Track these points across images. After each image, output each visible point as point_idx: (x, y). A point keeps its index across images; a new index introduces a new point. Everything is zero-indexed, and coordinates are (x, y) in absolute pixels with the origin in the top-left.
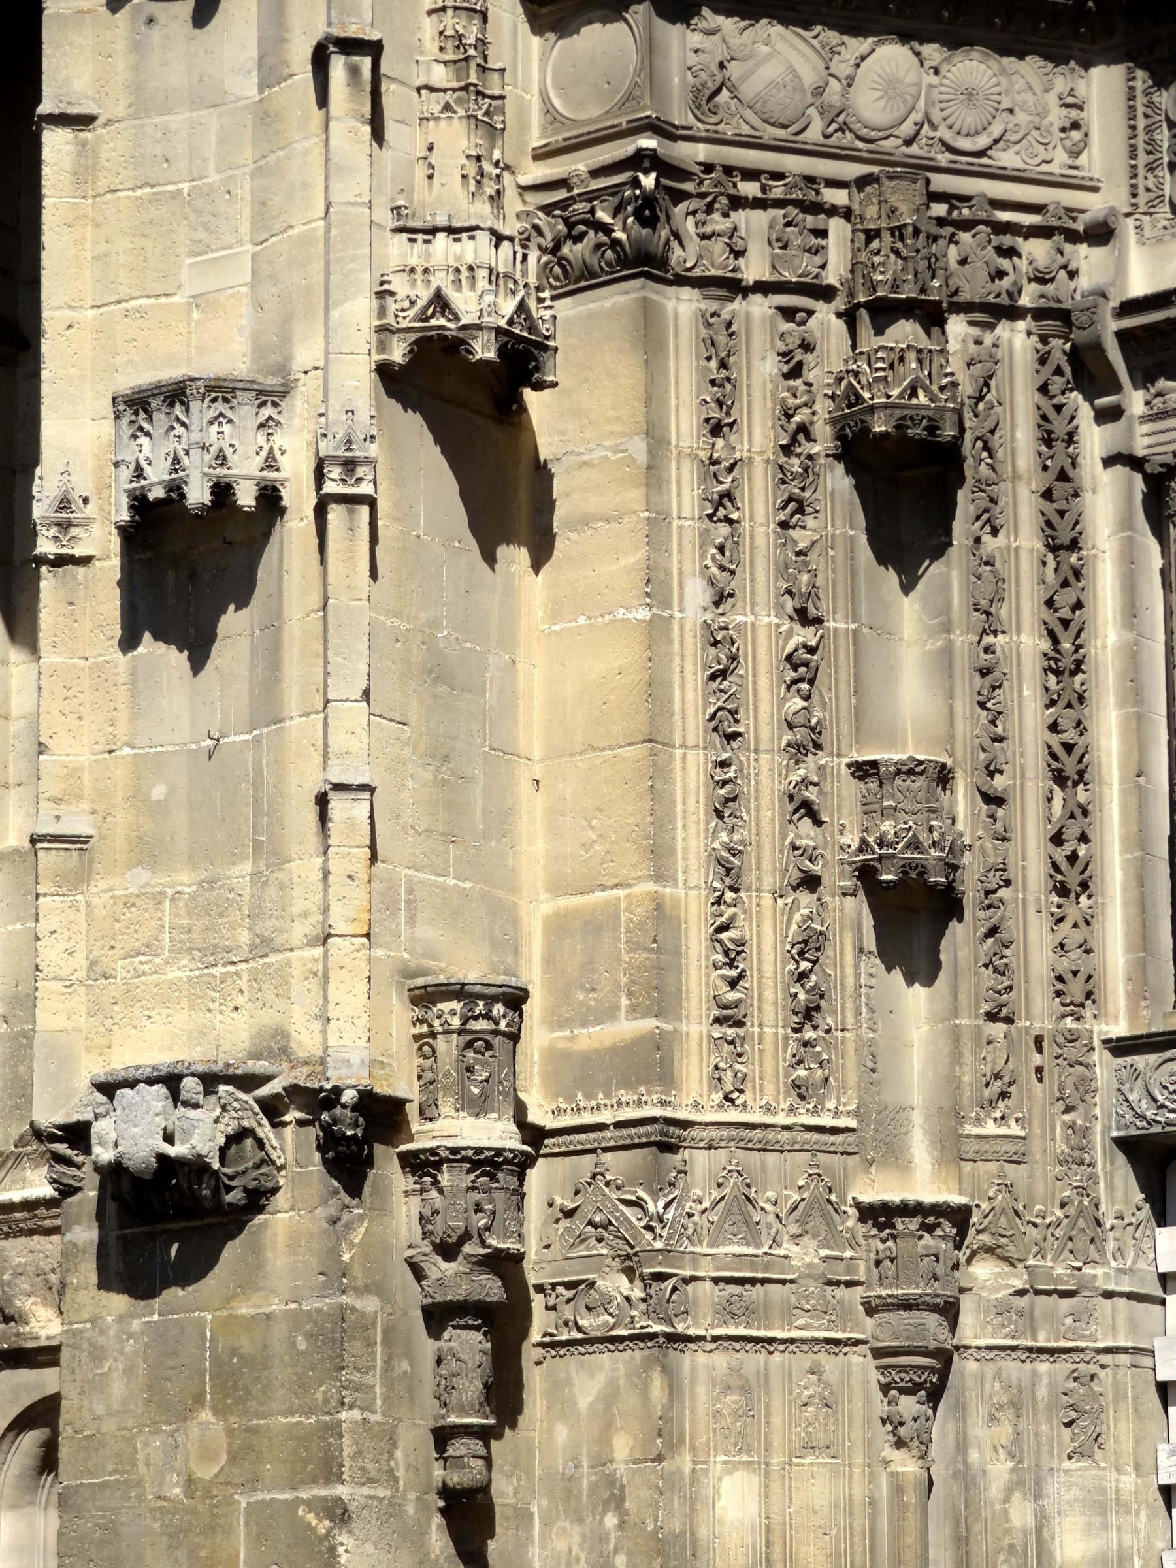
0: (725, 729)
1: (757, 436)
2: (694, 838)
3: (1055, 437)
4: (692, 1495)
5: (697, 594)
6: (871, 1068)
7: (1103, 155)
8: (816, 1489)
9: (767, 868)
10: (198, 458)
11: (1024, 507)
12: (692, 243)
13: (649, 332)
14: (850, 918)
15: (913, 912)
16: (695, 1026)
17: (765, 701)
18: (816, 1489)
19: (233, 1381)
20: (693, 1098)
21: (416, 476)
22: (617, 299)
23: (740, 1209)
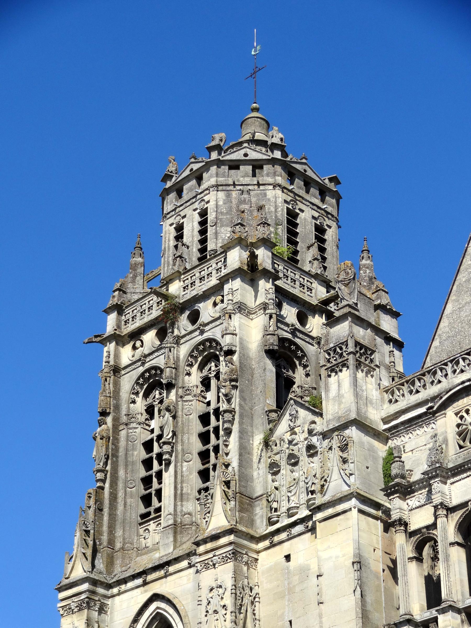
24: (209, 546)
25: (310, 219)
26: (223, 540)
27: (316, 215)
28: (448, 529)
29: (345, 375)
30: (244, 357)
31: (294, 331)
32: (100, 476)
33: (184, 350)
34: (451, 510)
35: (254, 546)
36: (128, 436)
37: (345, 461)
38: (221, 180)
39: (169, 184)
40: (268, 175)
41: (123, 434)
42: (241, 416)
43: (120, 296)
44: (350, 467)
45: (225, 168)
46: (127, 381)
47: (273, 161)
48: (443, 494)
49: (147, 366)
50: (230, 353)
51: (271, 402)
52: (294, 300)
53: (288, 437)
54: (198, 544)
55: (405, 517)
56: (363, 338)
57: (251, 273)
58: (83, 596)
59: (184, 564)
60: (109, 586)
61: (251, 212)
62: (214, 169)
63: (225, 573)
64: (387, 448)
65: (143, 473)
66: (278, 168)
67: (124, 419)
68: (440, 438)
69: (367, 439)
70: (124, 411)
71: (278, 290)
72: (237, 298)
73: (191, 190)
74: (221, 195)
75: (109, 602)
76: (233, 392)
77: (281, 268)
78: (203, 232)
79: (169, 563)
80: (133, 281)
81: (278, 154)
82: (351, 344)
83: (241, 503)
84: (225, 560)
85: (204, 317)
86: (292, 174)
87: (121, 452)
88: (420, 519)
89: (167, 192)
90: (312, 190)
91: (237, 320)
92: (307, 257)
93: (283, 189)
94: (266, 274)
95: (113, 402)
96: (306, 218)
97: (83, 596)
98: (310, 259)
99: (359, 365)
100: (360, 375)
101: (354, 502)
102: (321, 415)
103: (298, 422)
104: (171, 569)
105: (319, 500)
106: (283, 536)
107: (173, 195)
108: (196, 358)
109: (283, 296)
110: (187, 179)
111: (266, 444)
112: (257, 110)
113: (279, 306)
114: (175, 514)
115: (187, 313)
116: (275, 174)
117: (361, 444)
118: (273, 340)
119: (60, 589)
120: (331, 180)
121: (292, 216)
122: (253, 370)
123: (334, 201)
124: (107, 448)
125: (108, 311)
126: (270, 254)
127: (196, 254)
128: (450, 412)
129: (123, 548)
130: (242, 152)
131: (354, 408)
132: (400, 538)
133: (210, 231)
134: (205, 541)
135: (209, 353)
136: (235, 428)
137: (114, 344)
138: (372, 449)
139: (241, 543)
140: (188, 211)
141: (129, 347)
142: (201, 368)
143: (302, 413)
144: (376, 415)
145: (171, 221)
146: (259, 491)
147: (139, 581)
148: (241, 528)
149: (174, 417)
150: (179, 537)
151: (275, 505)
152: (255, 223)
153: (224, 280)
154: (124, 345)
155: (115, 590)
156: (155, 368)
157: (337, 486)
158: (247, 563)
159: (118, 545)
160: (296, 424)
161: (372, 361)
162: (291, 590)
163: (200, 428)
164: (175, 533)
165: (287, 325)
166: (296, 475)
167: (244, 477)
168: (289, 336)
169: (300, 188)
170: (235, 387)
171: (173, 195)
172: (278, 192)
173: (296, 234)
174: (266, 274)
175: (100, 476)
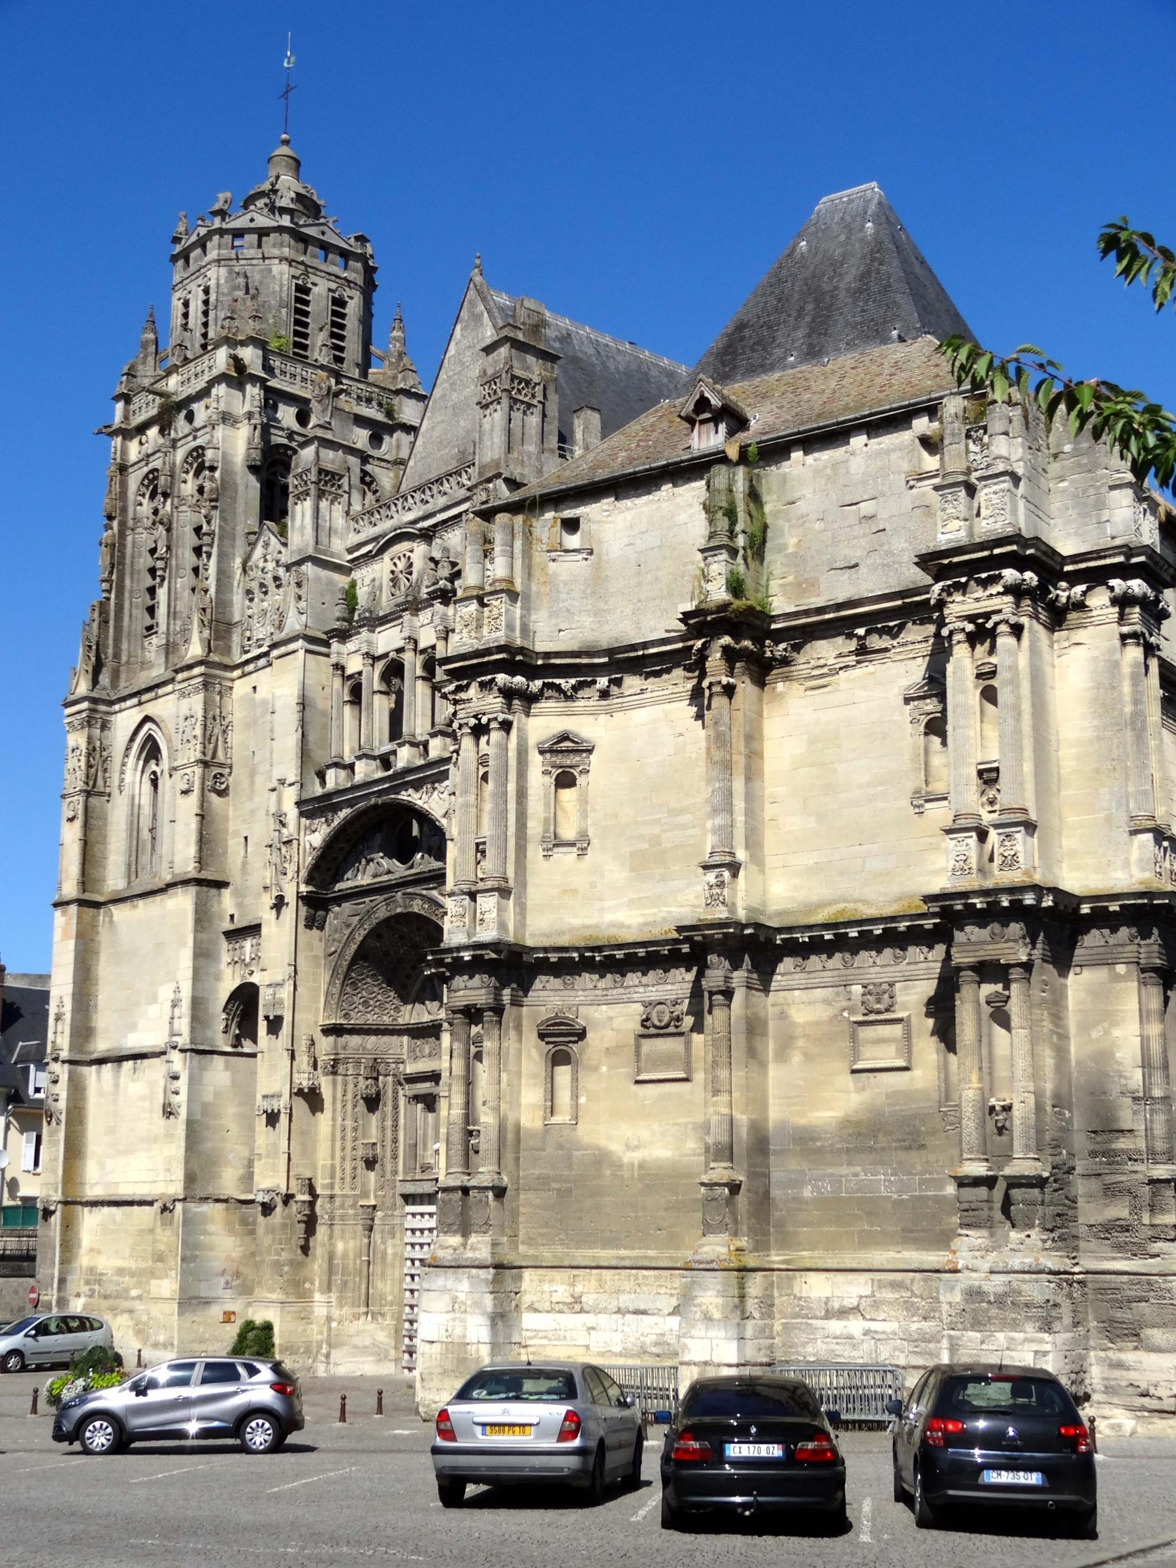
0: (343, 1138)
1: (350, 1096)
2: (338, 1154)
3: (395, 1092)
4: (332, 1245)
5: (339, 1120)
6: (363, 1185)
7: (405, 1050)
8: (352, 1244)
9: (348, 1159)
10: (267, 1105)
11: (390, 1103)
12: (341, 1069)
13: (334, 1083)
14: (361, 1165)
15: (370, 1164)
16: (337, 1180)
17: (349, 1134)
18: (352, 1244)
19: (273, 1231)
20: (337, 1191)
21: (301, 1106)
22: (330, 1077)
23: (342, 1206)
24: (185, 674)
25: (324, 292)
26: (197, 671)
27: (333, 286)
28: (373, 678)
29: (308, 504)
30: (228, 472)
31: (291, 435)
32: (105, 586)
33: (180, 454)
34: (375, 659)
35: (228, 675)
36: (134, 542)
37: (300, 598)
38: (224, 252)
39: (178, 248)
40: (274, 246)
41: (129, 539)
42: (221, 538)
43: (128, 381)
44: (303, 604)
45: (228, 238)
46: (134, 480)
47: (280, 229)
48: (369, 643)
49: (151, 466)
50: (212, 469)
51: (253, 522)
52: (291, 399)
53: (261, 564)
54: (176, 672)
55: (343, 662)
56: (333, 462)
57: (238, 376)
58: (84, 715)
59: (169, 688)
60: (111, 703)
61: (244, 300)
62: (216, 238)
63: (196, 703)
64: (349, 579)
65: (149, 582)
66: (286, 237)
67: (130, 523)
68: (377, 583)
69: (325, 574)
70: (130, 515)
71: (269, 391)
72: (222, 407)
73: (196, 260)
74: (223, 271)
75: (112, 718)
76: (213, 512)
77: (277, 363)
78: (206, 313)
79: (158, 686)
80: (144, 363)
81: (286, 221)
82: (314, 471)
83: (217, 631)
84: (197, 690)
85: (199, 420)
86: (304, 240)
87: (128, 561)
88: (354, 665)
89: (174, 259)
90: (330, 256)
91: (220, 432)
92: (318, 340)
93: (290, 262)
94: (254, 379)
95: (119, 504)
96: (320, 290)
97: (84, 715)
98: (319, 343)
99: (321, 494)
100: (324, 504)
101: (300, 643)
102: (285, 545)
103: (270, 549)
104: (161, 691)
105: (276, 638)
106: (251, 667)
107: (181, 263)
108: (191, 465)
109: (273, 398)
110: (193, 247)
111: (245, 571)
112: (286, 142)
113: (275, 408)
114: (168, 633)
115: (184, 412)
116: (282, 245)
117: (318, 579)
118: (256, 455)
119: (67, 705)
120: (357, 238)
121: (303, 290)
122: (236, 484)
123: (359, 265)
124: (112, 556)
125: (117, 398)
126: (260, 352)
127: (199, 340)
128: (386, 557)
129: (128, 662)
130: (248, 216)
131: (312, 542)
132: (337, 682)
133: (212, 314)
134: (182, 670)
135: (198, 462)
136: (215, 551)
137: (119, 439)
138: (330, 583)
139: (214, 673)
140: (192, 286)
141: (135, 442)
142: (197, 475)
143: (273, 540)
144: (339, 548)
145: (177, 295)
146: (237, 618)
147: (135, 701)
148: (214, 657)
149: (169, 530)
150: (171, 657)
151: (248, 634)
152: (247, 315)
153: (211, 383)
154: (131, 439)
155: (117, 707)
156: (156, 470)
157: (294, 623)
158: (220, 693)
159: (124, 659)
160: (269, 553)
161: (340, 487)
162: (255, 722)
163: (195, 541)
164: (167, 653)
165: (282, 429)
166: (265, 604)
167: (222, 602)
168: (285, 441)
169: (315, 256)
170: (215, 508)
171: (181, 263)
172: (285, 267)
173: (306, 314)
174: (254, 379)
175: (105, 586)
